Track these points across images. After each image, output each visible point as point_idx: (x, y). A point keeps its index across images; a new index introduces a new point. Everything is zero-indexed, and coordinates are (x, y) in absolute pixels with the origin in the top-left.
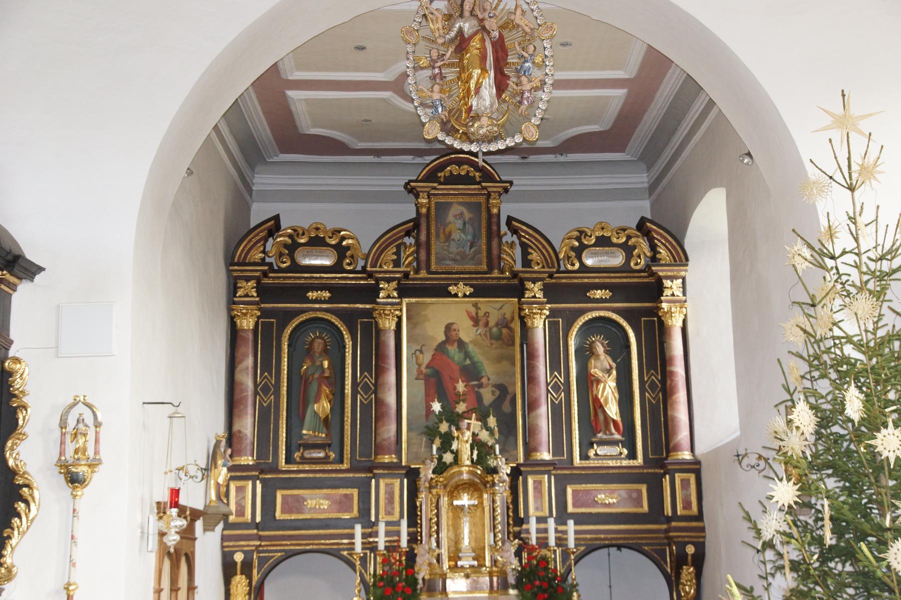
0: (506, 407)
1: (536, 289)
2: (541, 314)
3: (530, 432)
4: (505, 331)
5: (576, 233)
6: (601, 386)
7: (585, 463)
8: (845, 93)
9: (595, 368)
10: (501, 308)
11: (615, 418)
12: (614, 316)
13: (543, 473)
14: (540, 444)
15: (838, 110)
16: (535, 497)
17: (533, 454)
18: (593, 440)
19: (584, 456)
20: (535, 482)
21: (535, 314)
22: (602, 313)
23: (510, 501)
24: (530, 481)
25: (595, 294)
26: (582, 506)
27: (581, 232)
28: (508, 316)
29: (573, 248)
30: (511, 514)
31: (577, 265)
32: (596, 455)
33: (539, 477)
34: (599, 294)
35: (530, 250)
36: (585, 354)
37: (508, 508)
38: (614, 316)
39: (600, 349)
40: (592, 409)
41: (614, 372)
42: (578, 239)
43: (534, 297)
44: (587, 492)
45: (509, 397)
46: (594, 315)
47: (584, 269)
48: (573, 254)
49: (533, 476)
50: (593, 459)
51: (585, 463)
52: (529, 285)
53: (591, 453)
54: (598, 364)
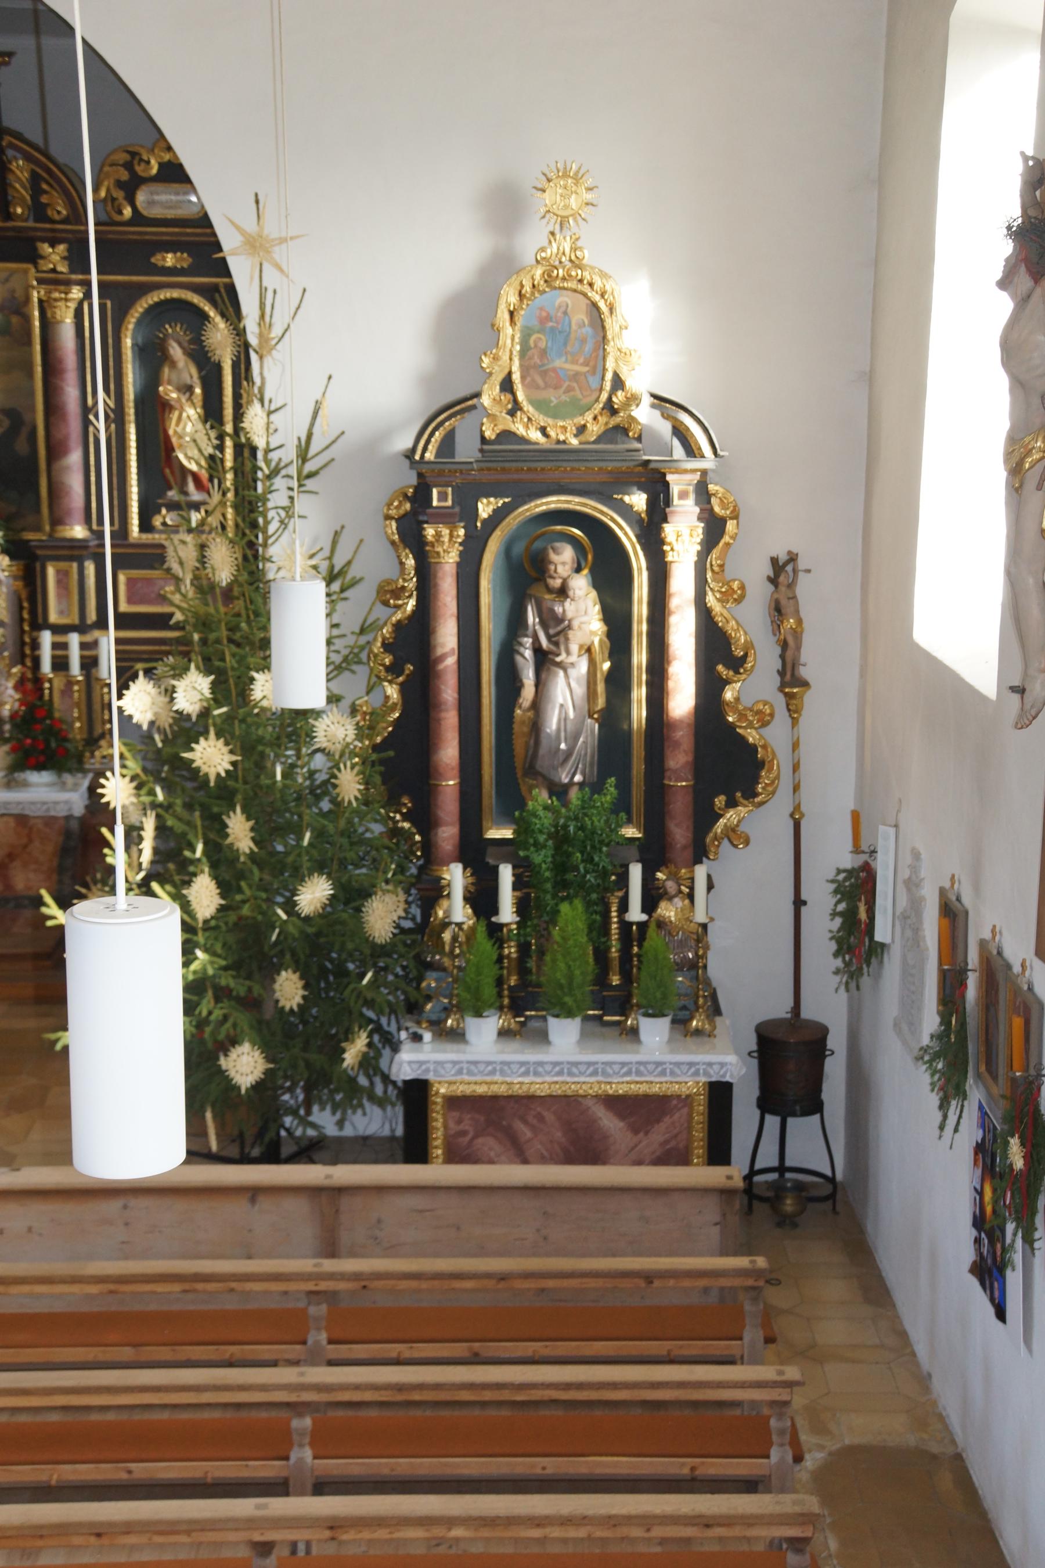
0: (21, 446)
1: (56, 258)
2: (66, 300)
3: (56, 492)
4: (15, 320)
5: (124, 157)
6: (175, 415)
7: (147, 537)
8: (260, 198)
9: (169, 383)
10: (7, 280)
11: (194, 467)
12: (196, 299)
13: (71, 558)
14: (69, 513)
15: (250, 225)
16: (59, 596)
17: (60, 528)
18: (160, 501)
19: (146, 526)
20: (58, 572)
21: (56, 300)
22: (175, 294)
23: (24, 596)
24: (51, 571)
25: (164, 259)
26: (141, 602)
27: (133, 154)
28: (19, 294)
29: (119, 184)
30: (26, 616)
31: (128, 212)
32: (164, 524)
33: (63, 565)
34: (170, 260)
35: (45, 186)
36: (152, 356)
37: (21, 608)
38: (196, 299)
39: (176, 351)
40: (157, 451)
41: (198, 391)
42: (129, 166)
43: (54, 271)
44: (149, 581)
45: (24, 432)
46: (162, 297)
47: (138, 218)
48: (119, 195)
49: (54, 563)
50: (161, 532)
51: (147, 537)
52: (46, 249)
53: (157, 521)
54: (174, 377)
